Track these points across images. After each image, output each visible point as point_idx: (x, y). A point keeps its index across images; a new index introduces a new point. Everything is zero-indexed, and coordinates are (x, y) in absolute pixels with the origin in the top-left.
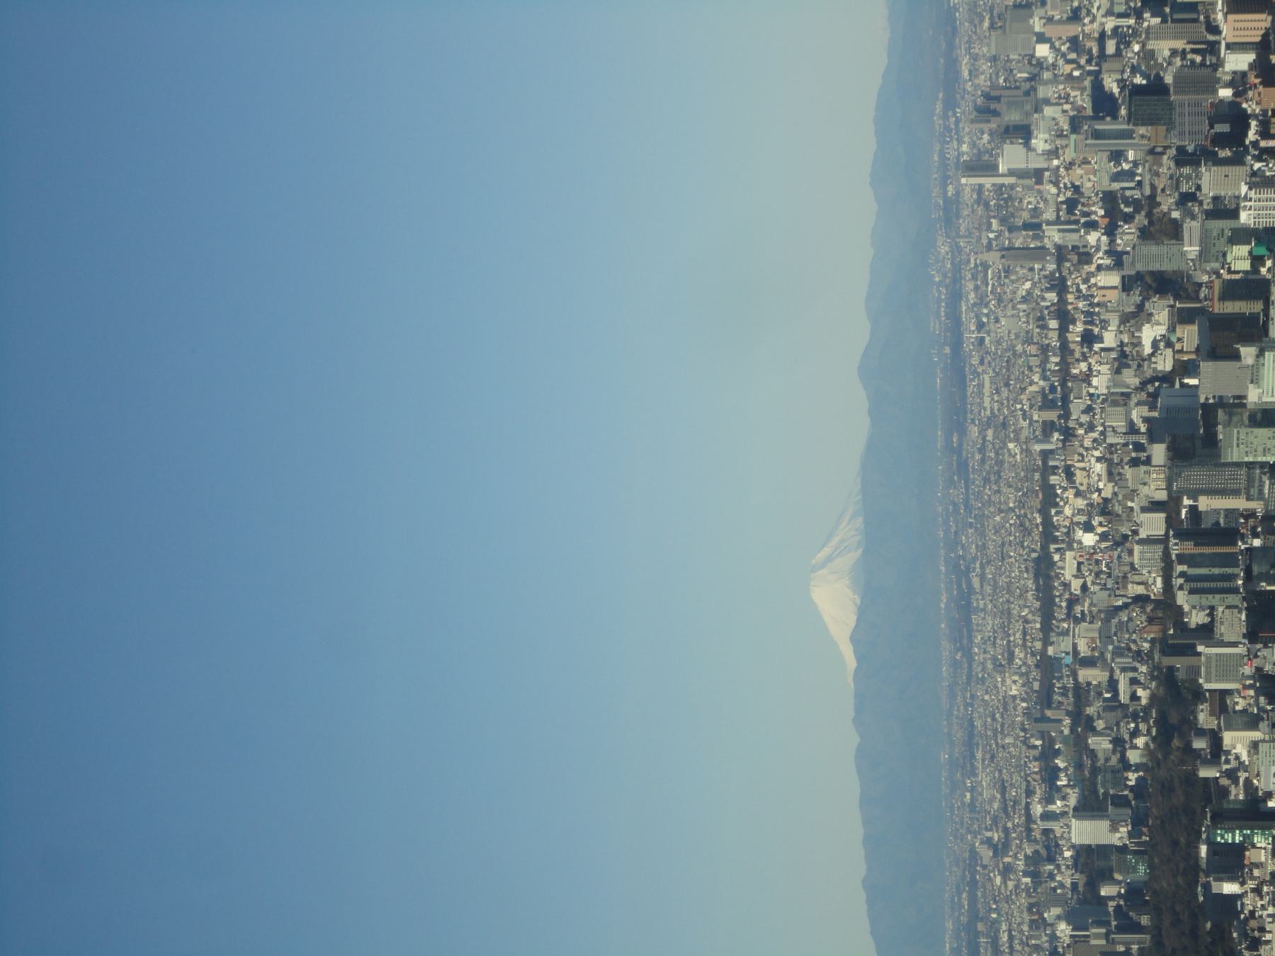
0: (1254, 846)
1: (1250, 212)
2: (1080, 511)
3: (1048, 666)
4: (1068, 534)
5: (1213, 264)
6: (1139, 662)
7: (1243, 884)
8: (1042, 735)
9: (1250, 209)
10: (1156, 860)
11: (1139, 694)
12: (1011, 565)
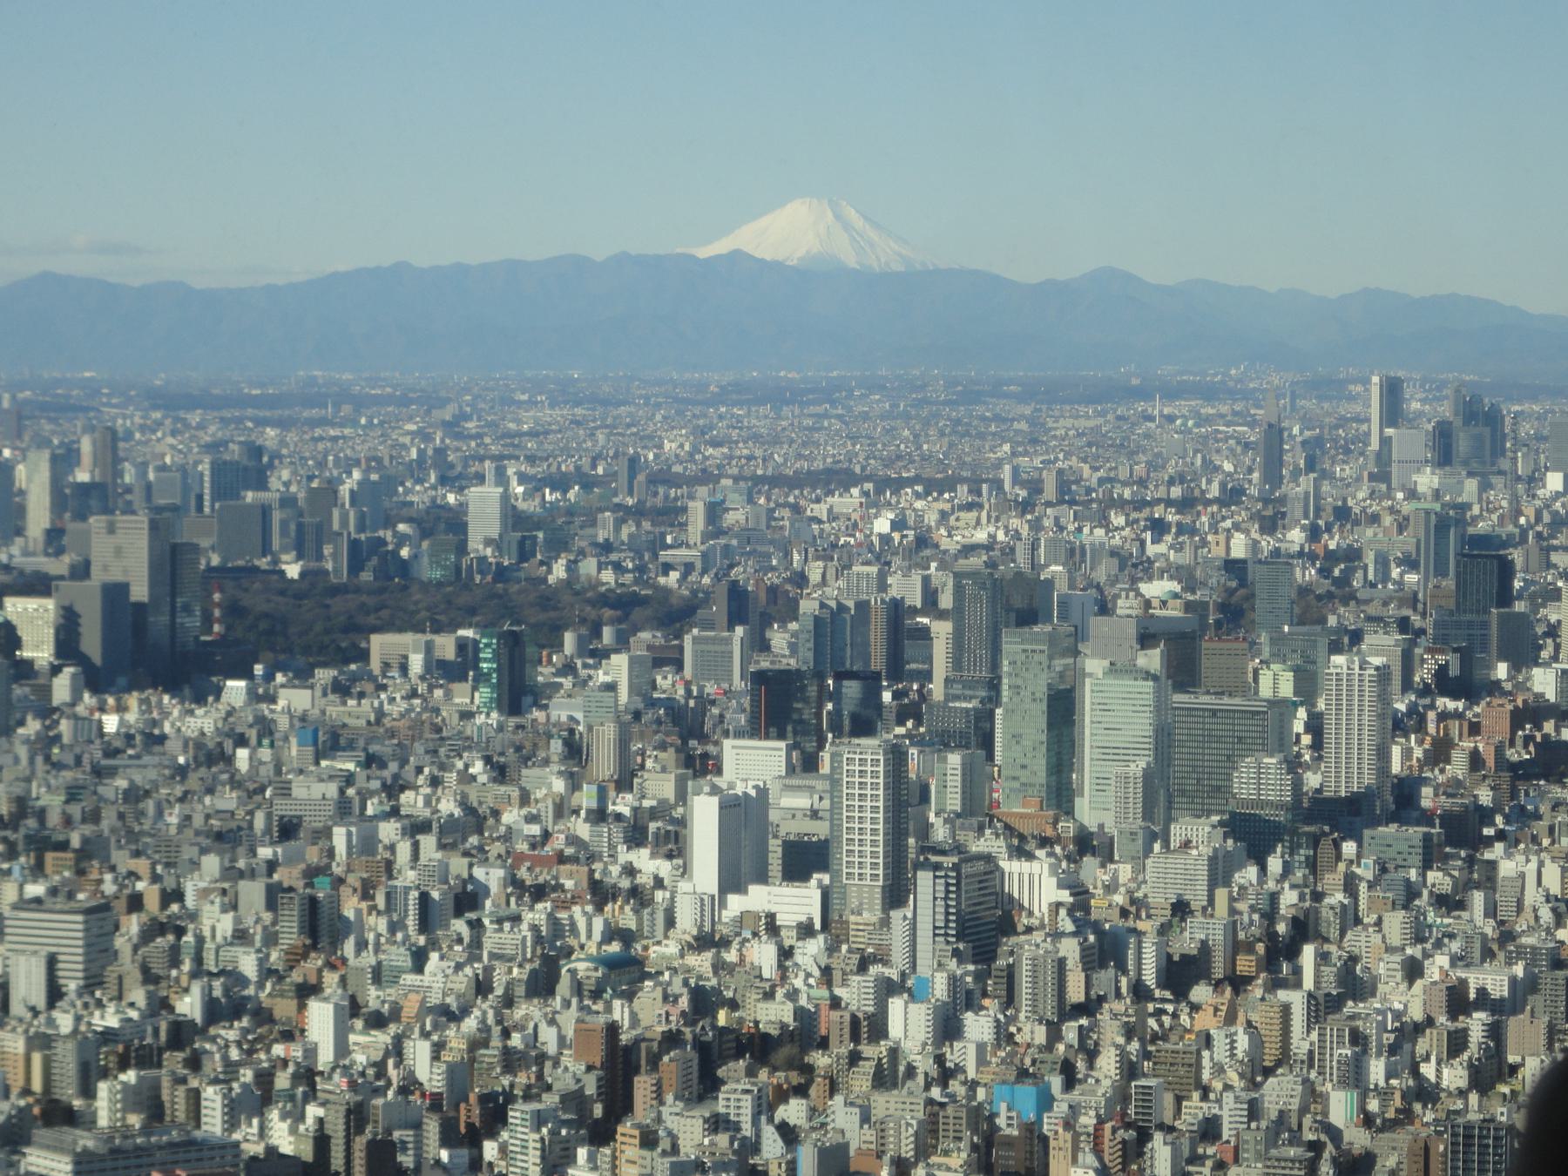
0: (475, 689)
1: (1345, 668)
2: (920, 517)
3: (707, 477)
4: (889, 504)
5: (1267, 649)
6: (716, 575)
7: (422, 678)
8: (611, 475)
9: (1349, 668)
10: (449, 589)
11: (671, 573)
12: (844, 445)
